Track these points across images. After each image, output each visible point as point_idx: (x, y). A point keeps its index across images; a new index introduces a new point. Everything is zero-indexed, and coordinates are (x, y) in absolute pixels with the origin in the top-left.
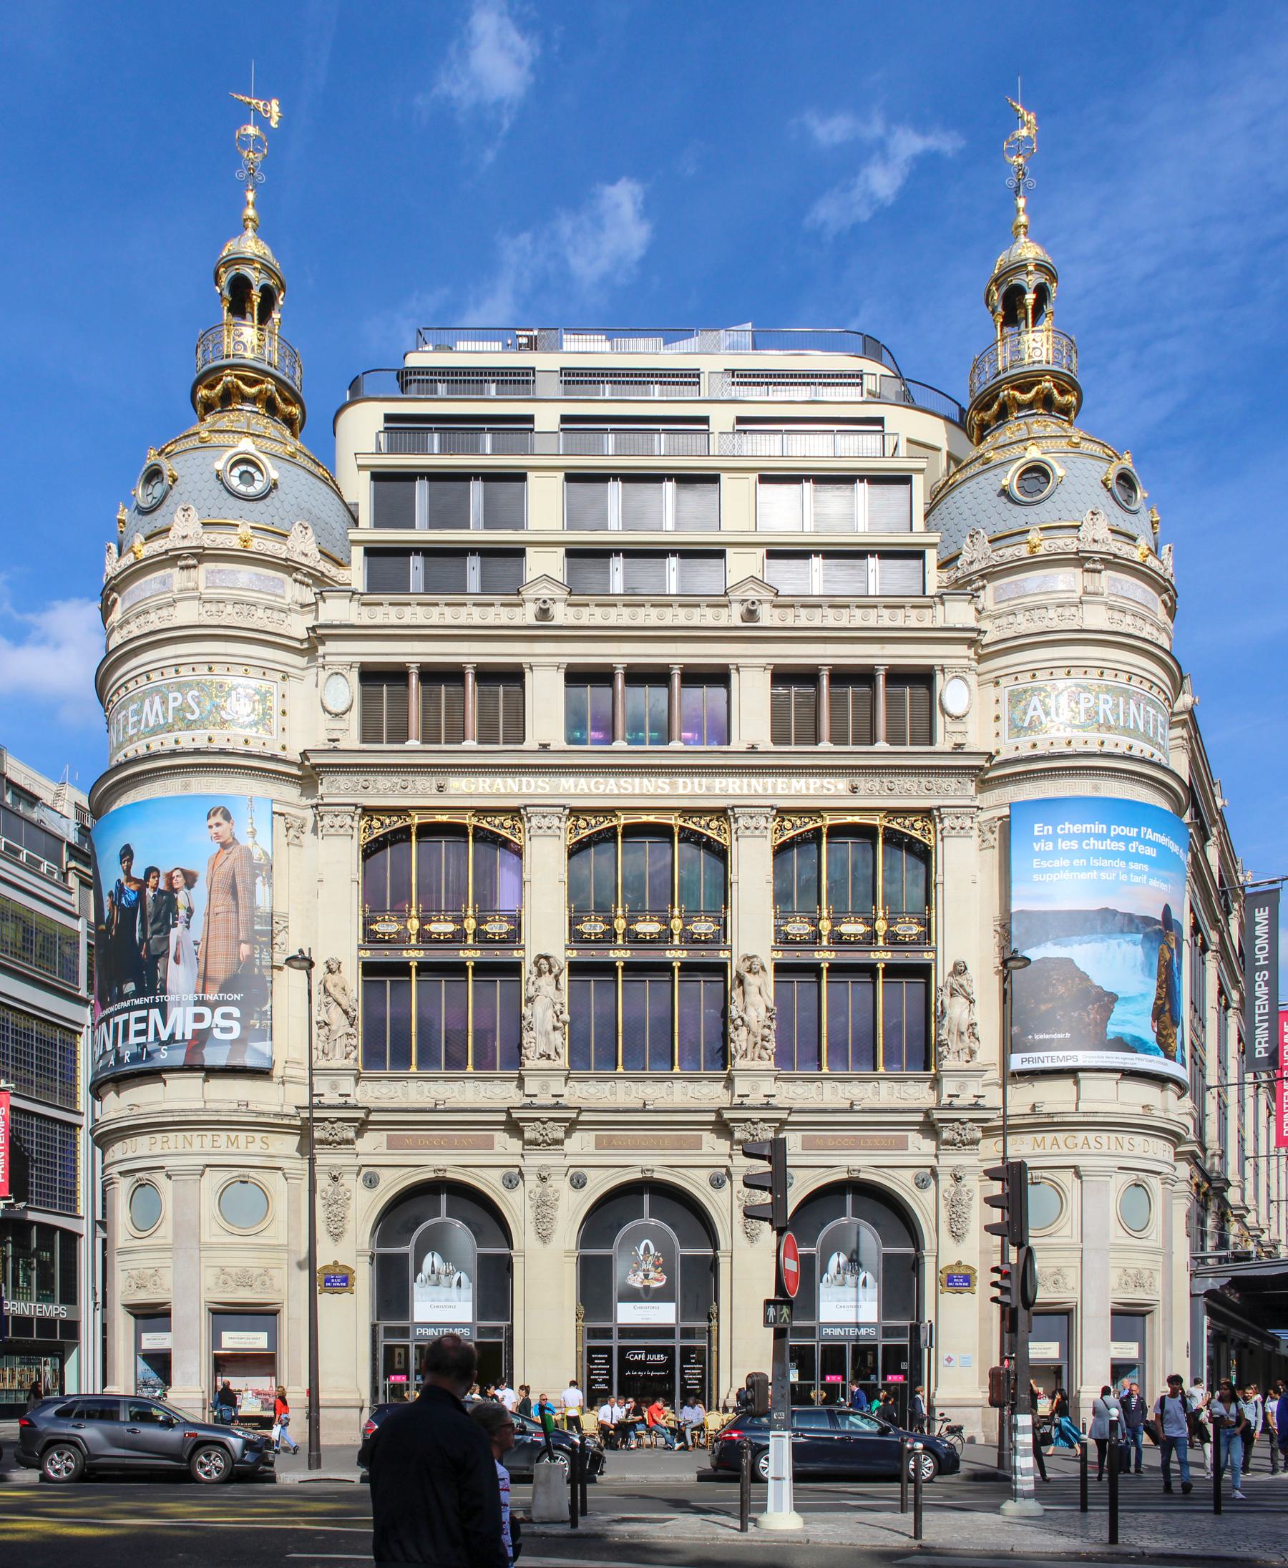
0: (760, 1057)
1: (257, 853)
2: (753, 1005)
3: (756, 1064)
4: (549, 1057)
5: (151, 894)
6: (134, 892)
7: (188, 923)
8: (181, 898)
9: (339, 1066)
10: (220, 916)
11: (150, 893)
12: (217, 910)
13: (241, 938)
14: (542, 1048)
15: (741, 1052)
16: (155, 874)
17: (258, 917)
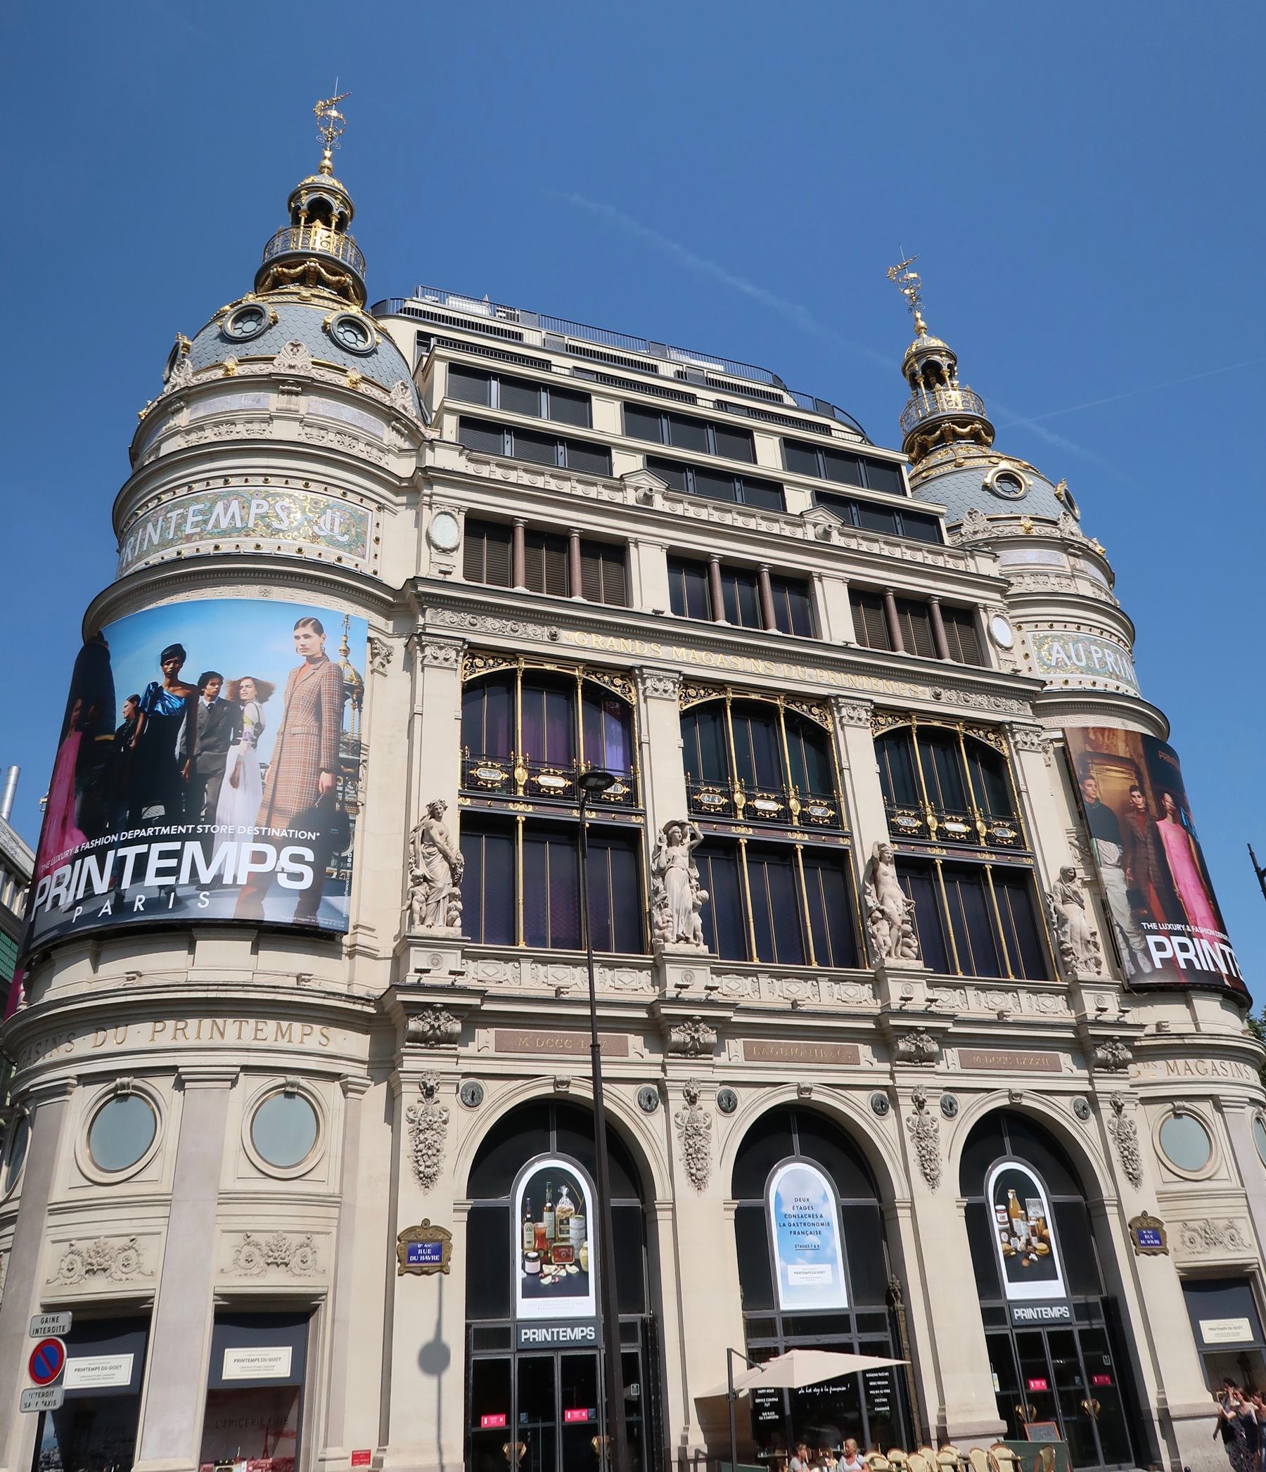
0: (903, 954)
1: (348, 674)
2: (891, 897)
3: (902, 963)
4: (687, 940)
5: (207, 703)
6: (179, 698)
7: (255, 741)
8: (249, 712)
9: (441, 935)
10: (297, 737)
11: (204, 701)
12: (295, 730)
13: (322, 765)
14: (681, 929)
15: (887, 948)
16: (215, 680)
17: (344, 743)
